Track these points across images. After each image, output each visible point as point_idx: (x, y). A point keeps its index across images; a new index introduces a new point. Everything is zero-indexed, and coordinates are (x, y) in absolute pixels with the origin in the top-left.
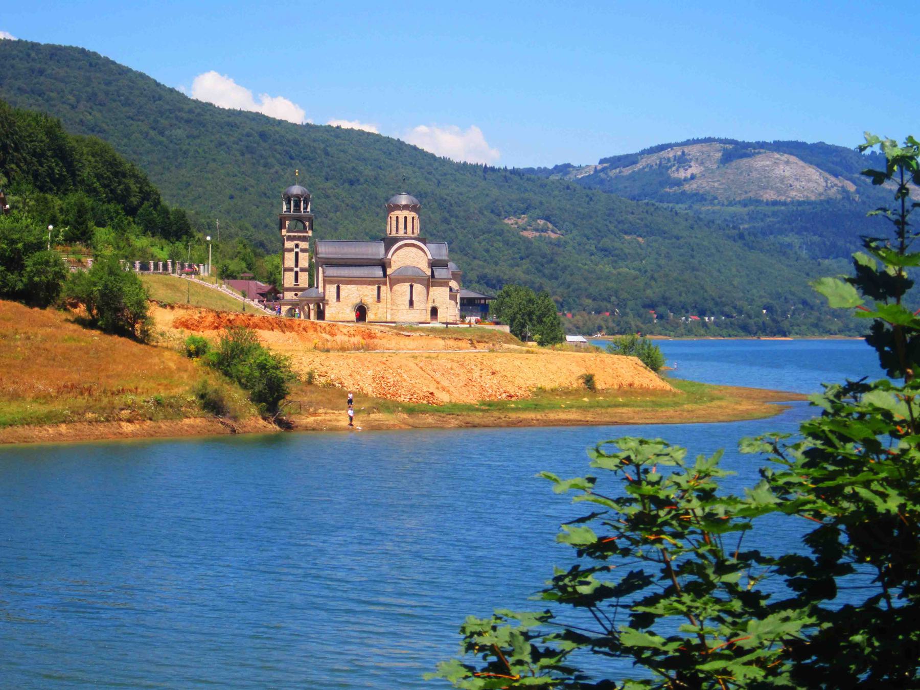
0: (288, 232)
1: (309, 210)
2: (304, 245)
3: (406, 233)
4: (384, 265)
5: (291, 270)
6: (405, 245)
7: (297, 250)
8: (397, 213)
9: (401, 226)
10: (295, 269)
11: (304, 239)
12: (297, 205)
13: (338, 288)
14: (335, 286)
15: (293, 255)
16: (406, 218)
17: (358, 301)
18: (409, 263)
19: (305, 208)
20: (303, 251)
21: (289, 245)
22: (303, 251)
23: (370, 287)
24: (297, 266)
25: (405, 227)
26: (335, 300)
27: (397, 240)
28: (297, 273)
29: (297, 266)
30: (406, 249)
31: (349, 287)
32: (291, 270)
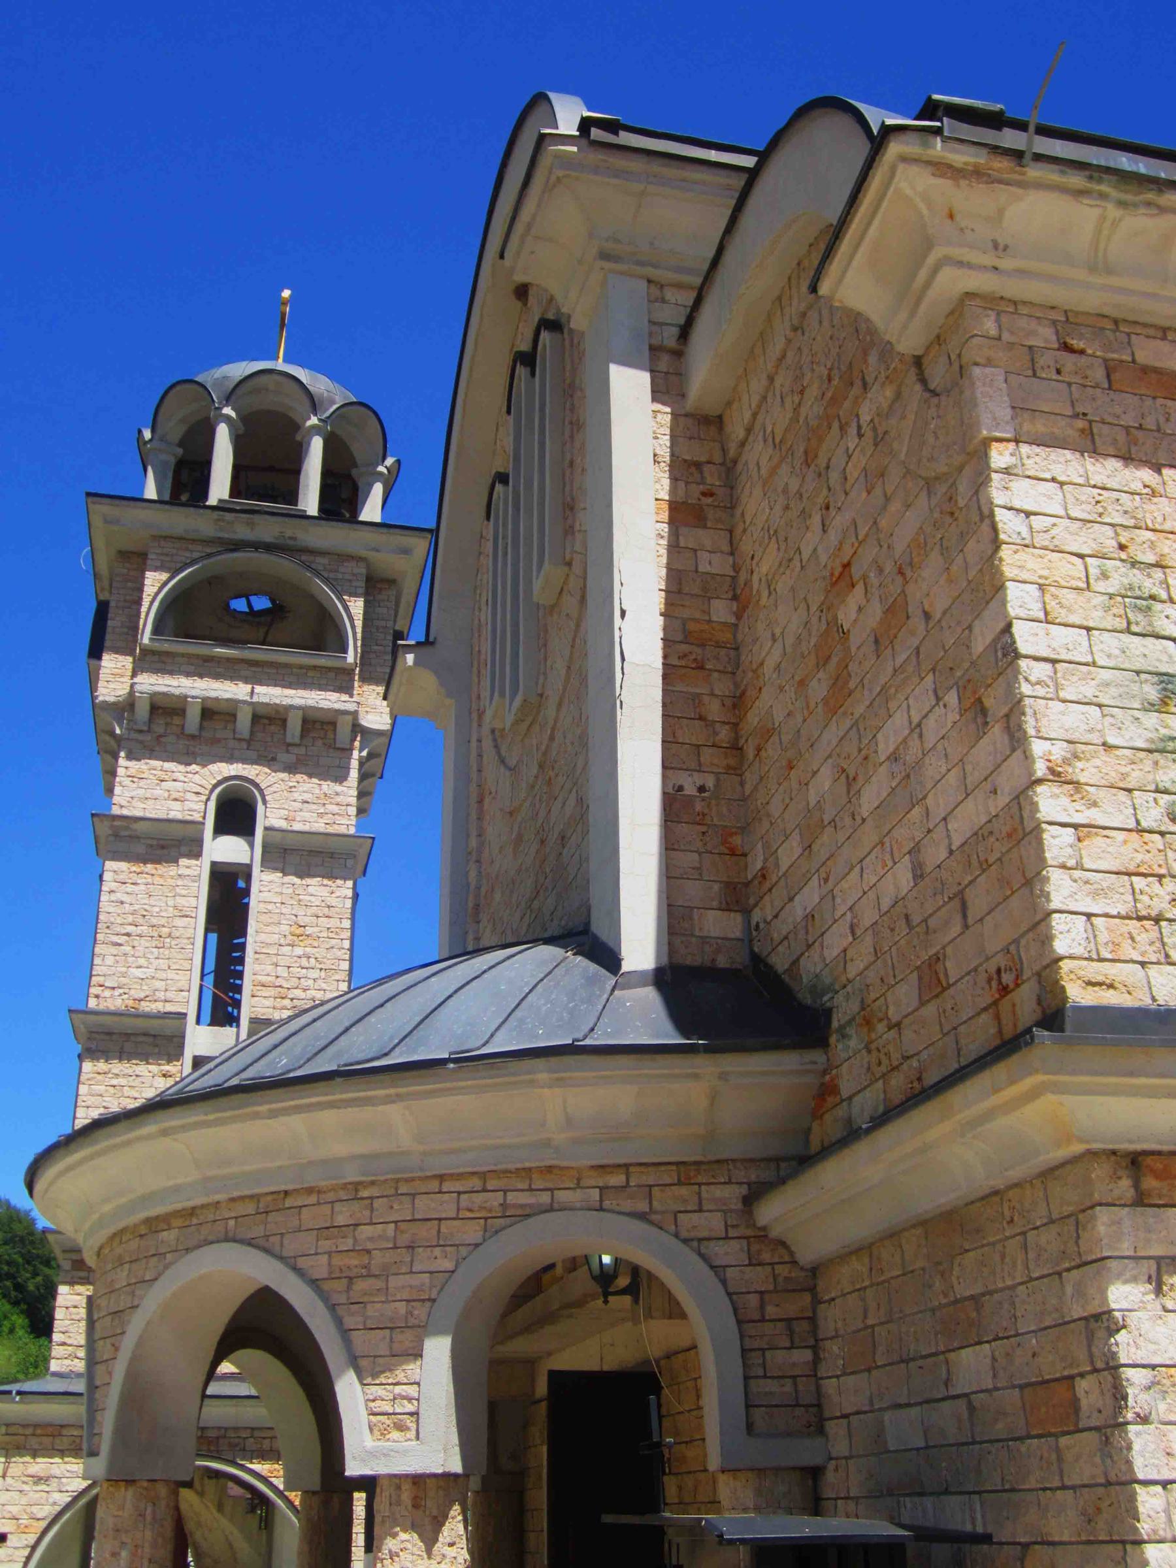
0: (148, 661)
2: (296, 802)
11: (314, 744)
12: (267, 471)
20: (300, 855)
21: (155, 789)
22: (300, 855)
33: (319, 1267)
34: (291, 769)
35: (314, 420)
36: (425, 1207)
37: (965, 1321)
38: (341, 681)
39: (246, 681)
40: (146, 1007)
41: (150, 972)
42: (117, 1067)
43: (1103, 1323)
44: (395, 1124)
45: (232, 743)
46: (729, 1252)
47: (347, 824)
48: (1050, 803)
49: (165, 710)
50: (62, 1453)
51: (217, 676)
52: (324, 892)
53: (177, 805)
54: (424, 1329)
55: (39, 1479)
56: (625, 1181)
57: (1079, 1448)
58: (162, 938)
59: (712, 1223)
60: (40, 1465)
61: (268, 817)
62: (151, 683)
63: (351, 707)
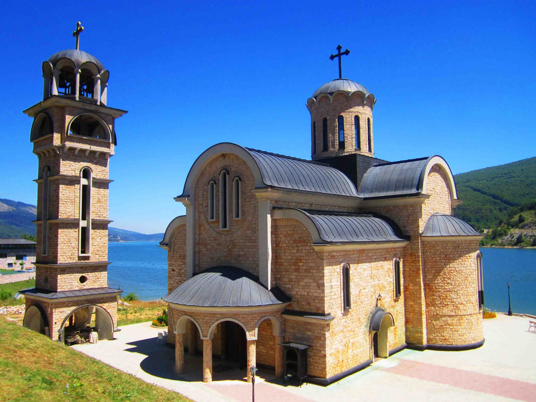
5: (72, 224)
13: (346, 273)
15: (76, 192)
21: (68, 168)
24: (85, 215)
28: (85, 231)
29: (85, 215)
32: (72, 224)
33: (243, 321)
34: (96, 164)
35: (99, 76)
36: (254, 316)
37: (309, 330)
39: (89, 144)
40: (71, 217)
41: (70, 210)
42: (66, 230)
43: (325, 335)
44: (254, 309)
45: (84, 157)
46: (280, 318)
47: (107, 177)
48: (326, 299)
50: (65, 307)
51: (83, 143)
52: (103, 192)
53: (74, 172)
54: (255, 327)
55: (61, 312)
56: (273, 313)
57: (321, 342)
58: (73, 202)
59: (278, 316)
60: (61, 309)
61: (93, 175)
62: (68, 144)
63: (109, 152)
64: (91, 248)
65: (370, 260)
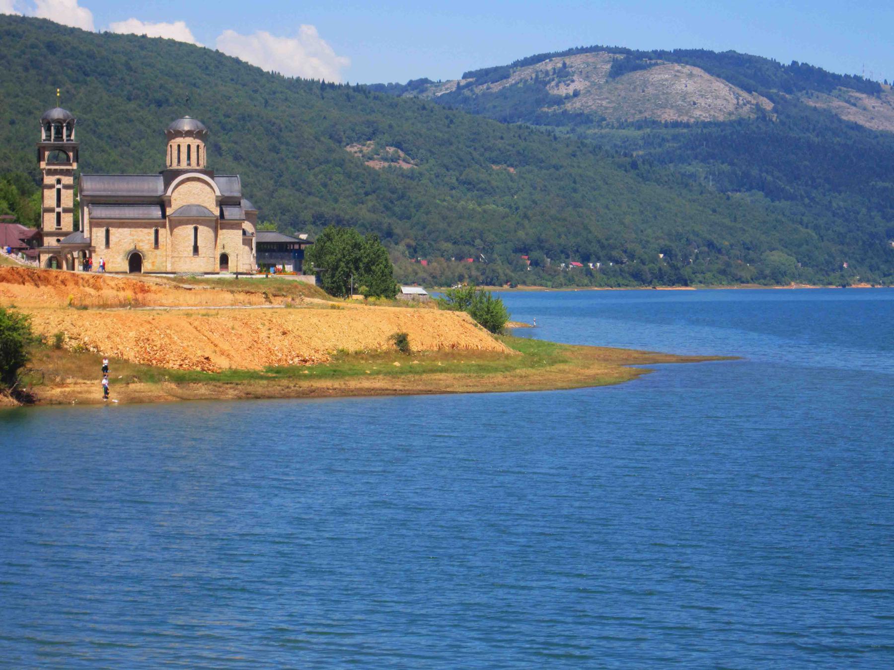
0: (48, 164)
1: (73, 137)
2: (68, 180)
3: (189, 164)
4: (162, 203)
5: (51, 210)
6: (188, 179)
7: (59, 186)
8: (179, 140)
9: (184, 156)
10: (57, 210)
11: (67, 173)
12: (59, 132)
13: (108, 232)
14: (104, 230)
15: (54, 192)
16: (189, 146)
17: (132, 247)
18: (193, 201)
19: (69, 136)
20: (67, 187)
21: (49, 180)
22: (67, 187)
23: (146, 231)
24: (59, 205)
25: (189, 158)
26: (103, 246)
27: (178, 173)
28: (59, 214)
29: (59, 205)
30: (189, 184)
31: (121, 230)
32: (51, 210)
38: (71, 165)
49: (49, 170)
61: (63, 182)
64: (62, 223)
65: (130, 227)
